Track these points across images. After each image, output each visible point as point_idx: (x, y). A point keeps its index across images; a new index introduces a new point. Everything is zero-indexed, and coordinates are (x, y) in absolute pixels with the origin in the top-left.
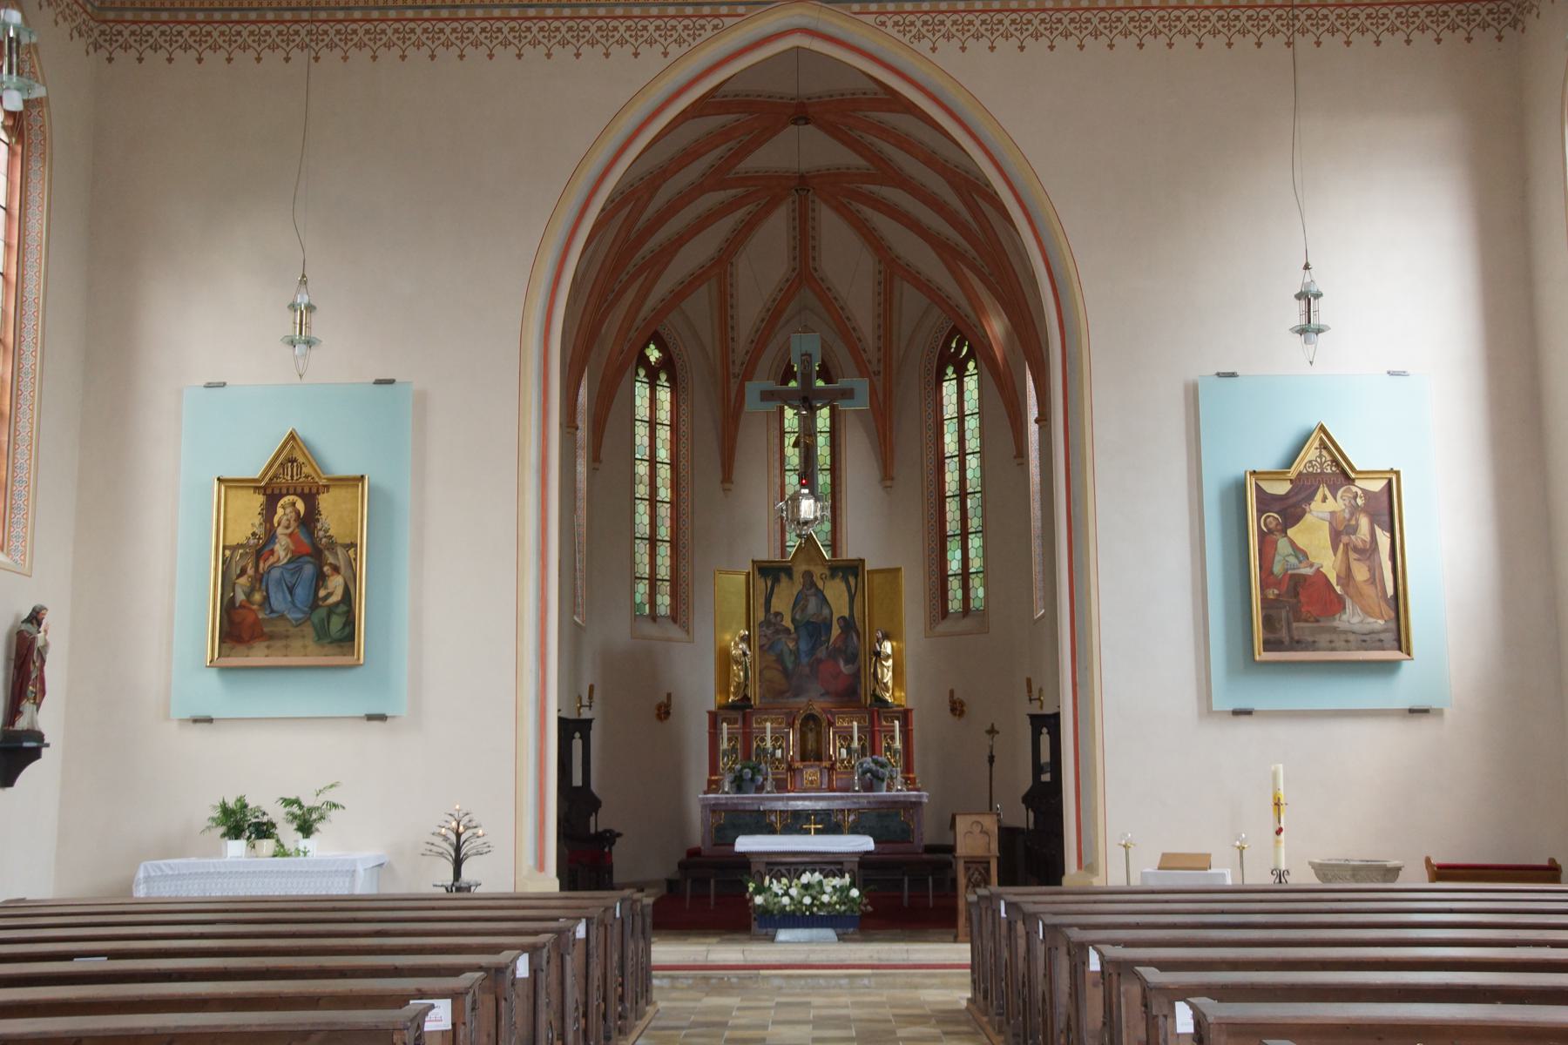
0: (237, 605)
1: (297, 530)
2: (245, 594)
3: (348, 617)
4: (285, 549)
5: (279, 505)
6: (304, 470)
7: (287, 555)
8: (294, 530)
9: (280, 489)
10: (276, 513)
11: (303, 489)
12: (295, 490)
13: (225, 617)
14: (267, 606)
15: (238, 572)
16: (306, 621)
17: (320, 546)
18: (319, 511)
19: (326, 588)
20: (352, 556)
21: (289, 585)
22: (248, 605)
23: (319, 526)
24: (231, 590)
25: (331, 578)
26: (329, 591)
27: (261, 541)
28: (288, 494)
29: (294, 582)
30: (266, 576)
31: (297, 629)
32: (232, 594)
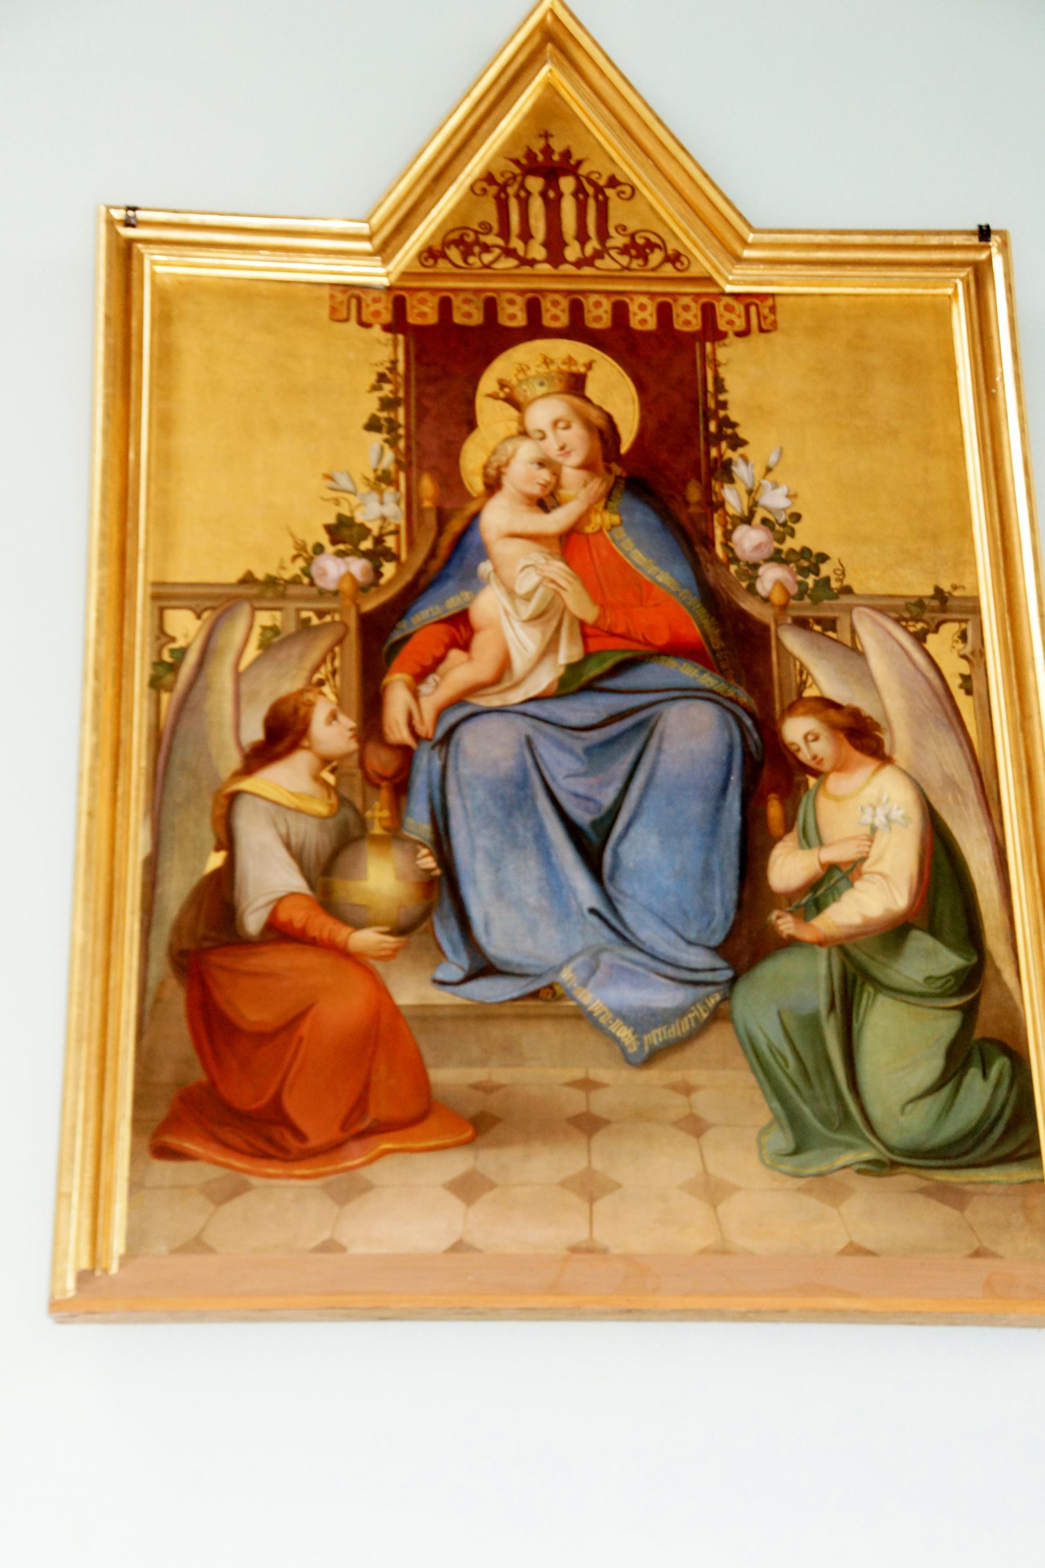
0: (253, 922)
1: (603, 519)
2: (298, 855)
3: (969, 1013)
4: (537, 617)
5: (488, 383)
6: (618, 212)
7: (551, 647)
8: (584, 518)
9: (491, 306)
10: (471, 425)
11: (620, 311)
12: (576, 309)
13: (176, 997)
14: (446, 933)
15: (254, 732)
16: (701, 1029)
17: (750, 606)
18: (727, 423)
19: (811, 839)
20: (953, 667)
21: (583, 817)
22: (322, 926)
23: (733, 498)
24: (207, 835)
25: (836, 783)
26: (829, 855)
27: (389, 569)
28: (535, 329)
29: (607, 797)
30: (426, 763)
31: (653, 1075)
32: (216, 860)
